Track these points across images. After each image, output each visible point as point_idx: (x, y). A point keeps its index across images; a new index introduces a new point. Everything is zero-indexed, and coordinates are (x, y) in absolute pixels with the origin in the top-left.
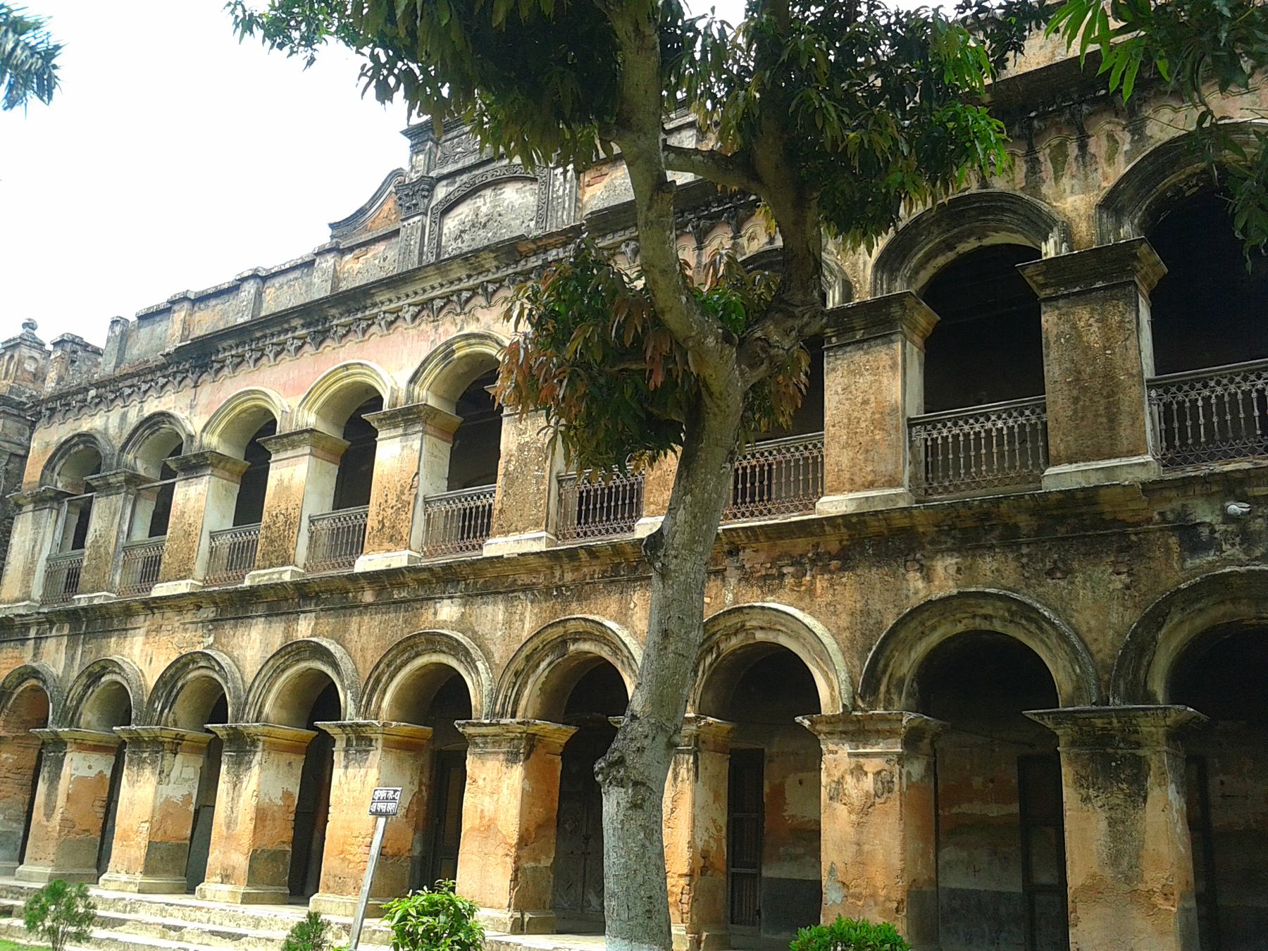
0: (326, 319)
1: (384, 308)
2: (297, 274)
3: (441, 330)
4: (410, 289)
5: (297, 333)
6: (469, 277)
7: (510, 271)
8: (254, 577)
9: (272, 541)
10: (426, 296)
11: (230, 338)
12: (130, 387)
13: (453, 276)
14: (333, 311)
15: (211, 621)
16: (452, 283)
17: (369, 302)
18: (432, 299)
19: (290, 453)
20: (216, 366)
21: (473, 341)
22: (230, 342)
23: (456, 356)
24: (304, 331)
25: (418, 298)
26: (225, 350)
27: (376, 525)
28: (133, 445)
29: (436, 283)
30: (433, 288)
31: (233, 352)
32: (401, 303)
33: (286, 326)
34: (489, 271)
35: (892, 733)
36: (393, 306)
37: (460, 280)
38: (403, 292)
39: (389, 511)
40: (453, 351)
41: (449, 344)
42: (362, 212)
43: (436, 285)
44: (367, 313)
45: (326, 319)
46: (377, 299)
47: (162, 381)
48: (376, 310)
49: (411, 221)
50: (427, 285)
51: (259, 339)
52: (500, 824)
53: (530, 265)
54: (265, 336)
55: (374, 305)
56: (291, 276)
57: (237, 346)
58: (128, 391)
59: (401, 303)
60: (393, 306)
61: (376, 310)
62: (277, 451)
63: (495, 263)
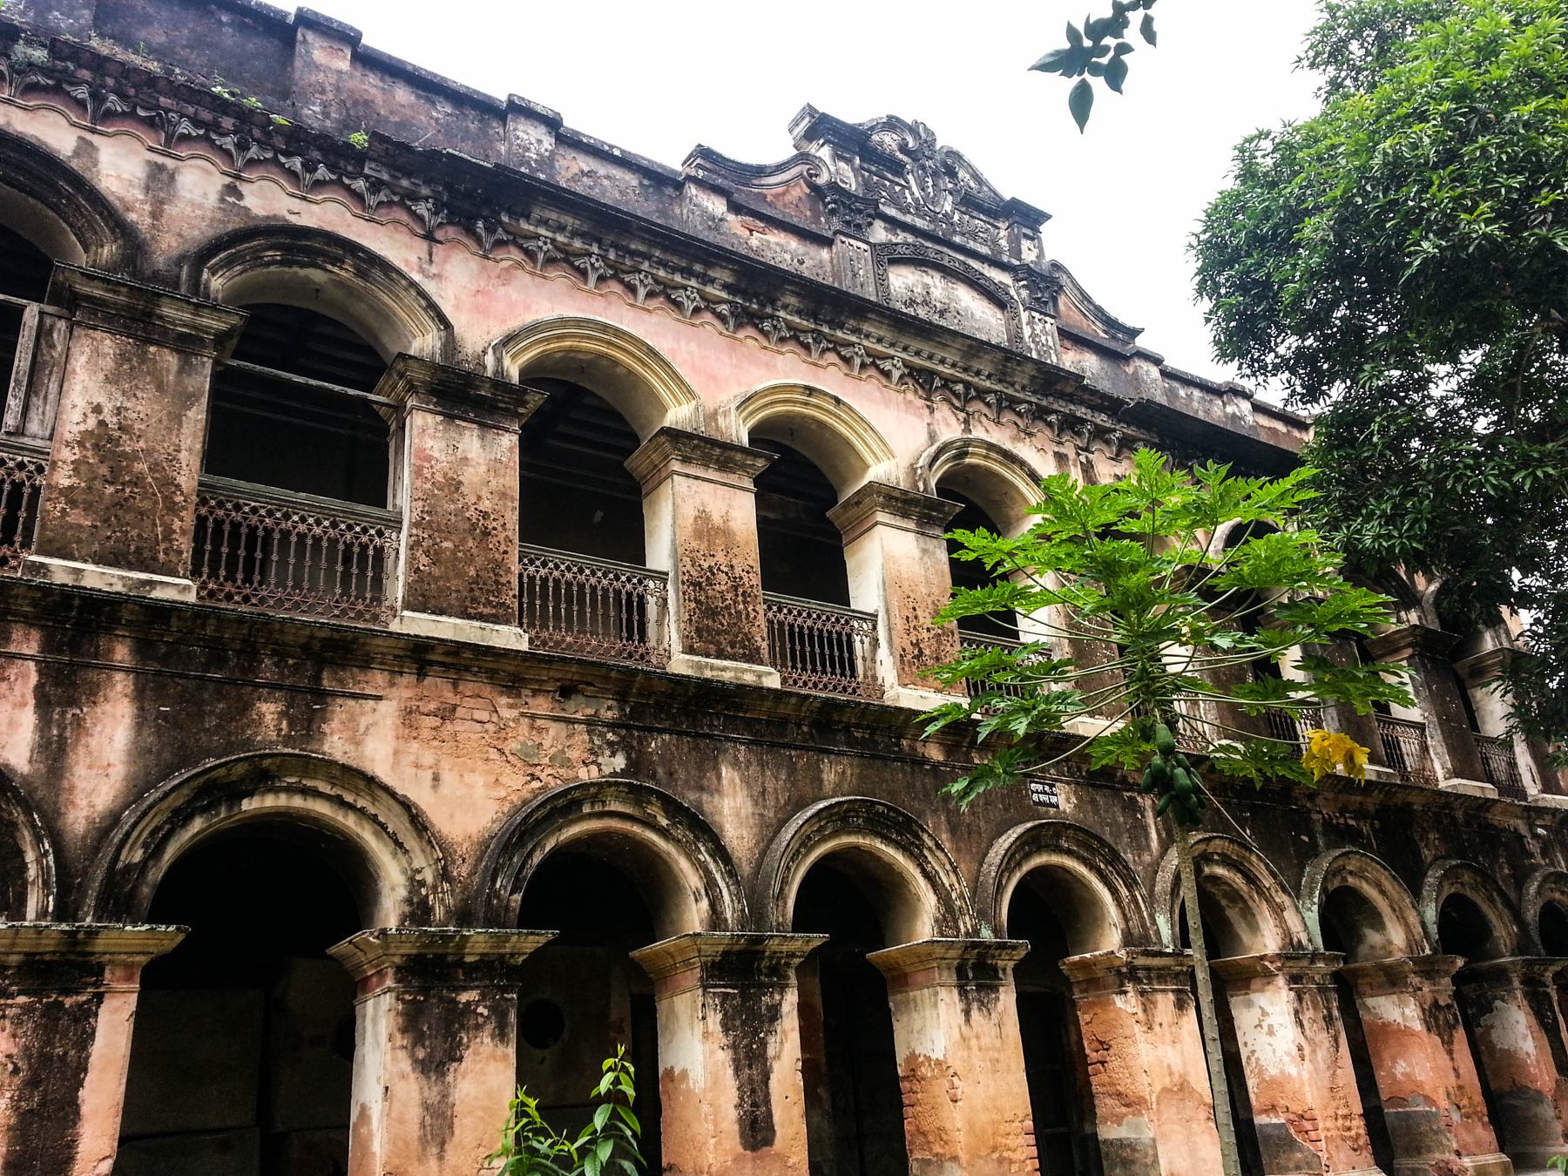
0: (773, 302)
1: (865, 343)
2: (632, 180)
3: (937, 414)
4: (915, 345)
5: (713, 291)
6: (989, 377)
7: (1034, 399)
8: (699, 667)
9: (712, 613)
10: (928, 364)
11: (576, 215)
12: (197, 123)
13: (976, 365)
14: (792, 300)
15: (612, 726)
16: (965, 370)
17: (852, 323)
18: (932, 373)
19: (712, 474)
20: (501, 234)
21: (994, 455)
22: (569, 220)
23: (967, 460)
24: (724, 295)
25: (916, 360)
26: (544, 222)
27: (909, 648)
28: (228, 263)
29: (950, 359)
30: (942, 362)
31: (560, 238)
32: (891, 352)
33: (698, 268)
34: (1013, 385)
35: (1447, 973)
36: (879, 347)
37: (978, 373)
38: (905, 341)
39: (925, 635)
40: (966, 453)
41: (968, 443)
42: (760, 171)
43: (950, 359)
44: (839, 334)
45: (773, 302)
46: (866, 327)
47: (322, 172)
48: (853, 339)
49: (852, 241)
50: (940, 354)
51: (633, 253)
52: (1192, 1080)
53: (1055, 406)
54: (647, 257)
55: (855, 331)
56: (617, 173)
57: (574, 234)
58: (185, 127)
59: (891, 352)
60: (879, 347)
61: (853, 339)
62: (686, 460)
63: (1025, 382)
